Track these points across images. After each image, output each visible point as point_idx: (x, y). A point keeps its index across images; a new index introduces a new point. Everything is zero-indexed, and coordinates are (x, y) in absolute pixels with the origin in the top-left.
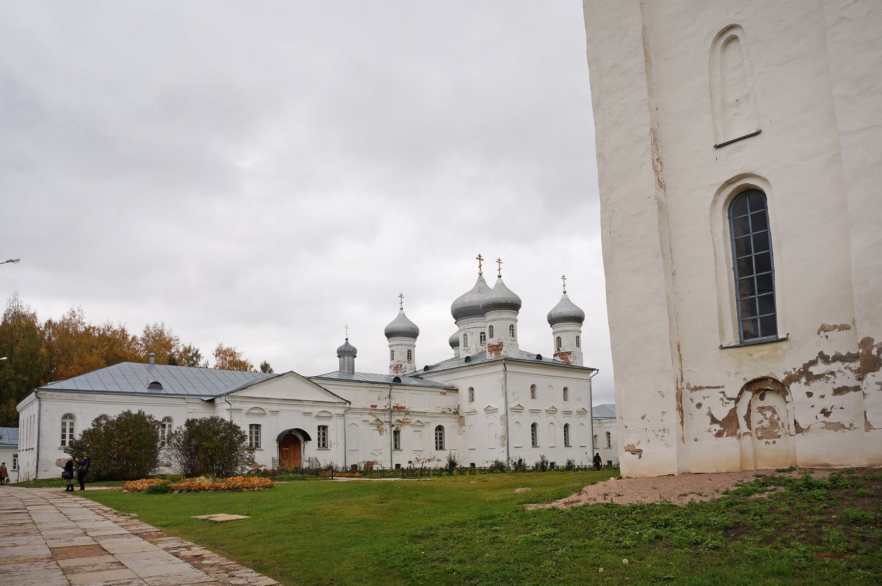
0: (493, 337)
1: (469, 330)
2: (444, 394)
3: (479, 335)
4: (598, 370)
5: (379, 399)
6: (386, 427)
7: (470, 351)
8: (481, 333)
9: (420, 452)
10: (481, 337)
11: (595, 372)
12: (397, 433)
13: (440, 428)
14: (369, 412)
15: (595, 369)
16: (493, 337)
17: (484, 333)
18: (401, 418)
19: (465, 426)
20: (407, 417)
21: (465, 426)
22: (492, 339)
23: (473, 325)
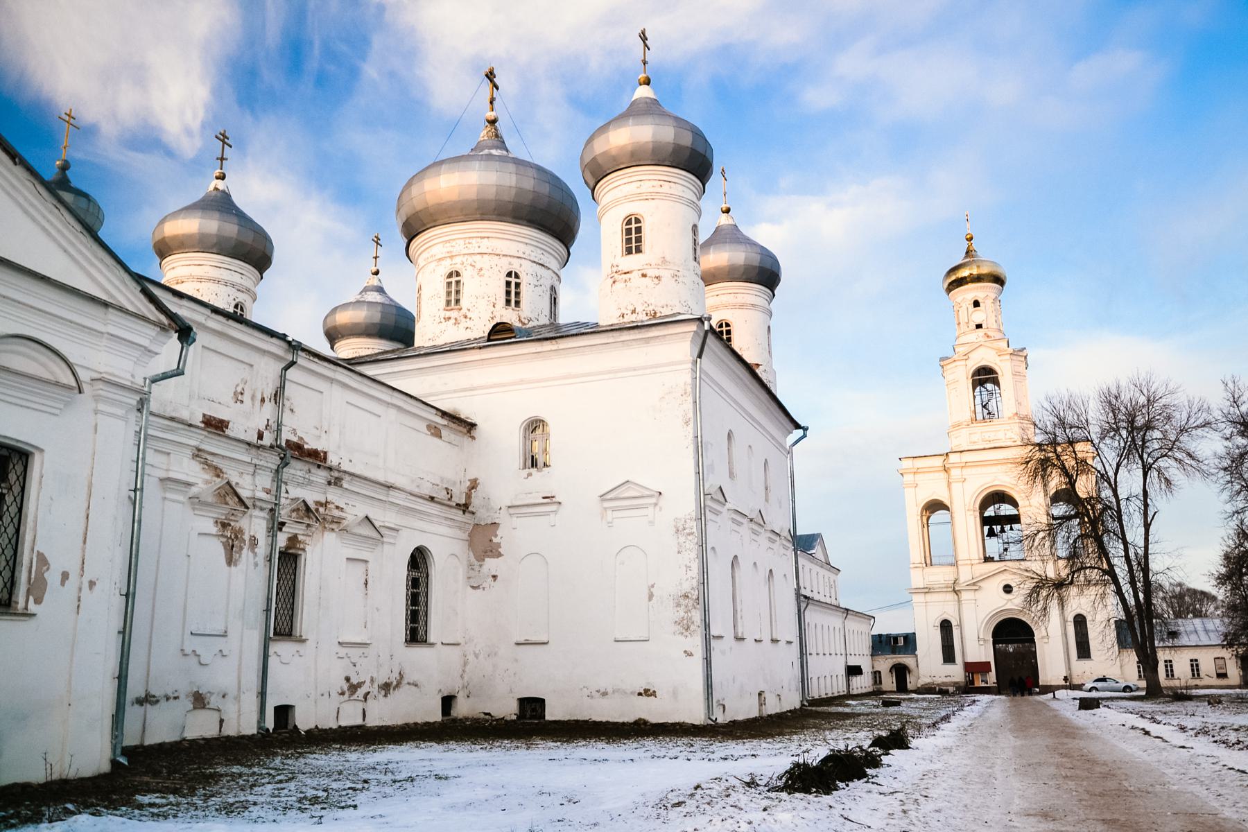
0: (639, 250)
1: (470, 259)
2: (435, 432)
3: (503, 279)
4: (805, 429)
5: (238, 397)
6: (255, 525)
7: (469, 324)
8: (509, 274)
9: (360, 651)
10: (508, 284)
11: (800, 432)
12: (289, 560)
13: (419, 559)
14: (194, 443)
15: (797, 426)
16: (639, 250)
17: (517, 276)
18: (311, 497)
19: (500, 555)
20: (334, 495)
21: (500, 555)
22: (634, 257)
23: (486, 245)
